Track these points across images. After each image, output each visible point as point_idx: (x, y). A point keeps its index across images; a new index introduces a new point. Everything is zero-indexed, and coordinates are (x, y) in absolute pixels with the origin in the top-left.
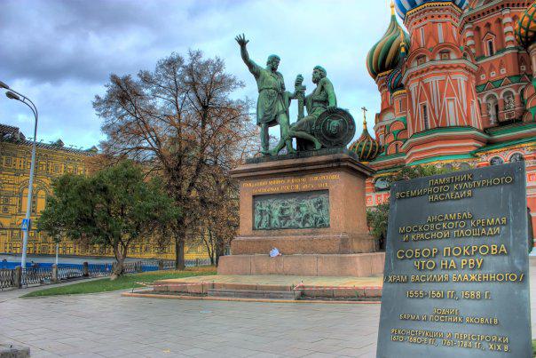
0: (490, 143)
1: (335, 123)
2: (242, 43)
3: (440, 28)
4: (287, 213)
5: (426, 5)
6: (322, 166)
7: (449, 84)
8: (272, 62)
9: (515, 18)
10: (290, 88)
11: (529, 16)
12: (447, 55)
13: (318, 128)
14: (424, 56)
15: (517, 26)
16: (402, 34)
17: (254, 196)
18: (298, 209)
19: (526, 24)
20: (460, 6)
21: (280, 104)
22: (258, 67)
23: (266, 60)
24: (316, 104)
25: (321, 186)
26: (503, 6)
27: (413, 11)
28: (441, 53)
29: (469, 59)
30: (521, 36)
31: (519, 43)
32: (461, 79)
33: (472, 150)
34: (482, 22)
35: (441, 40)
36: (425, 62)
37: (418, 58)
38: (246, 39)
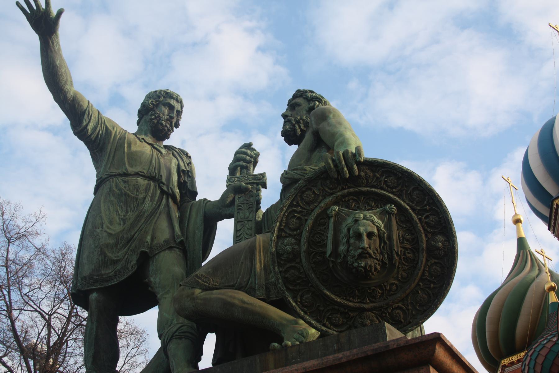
2: (44, 24)
10: (211, 187)
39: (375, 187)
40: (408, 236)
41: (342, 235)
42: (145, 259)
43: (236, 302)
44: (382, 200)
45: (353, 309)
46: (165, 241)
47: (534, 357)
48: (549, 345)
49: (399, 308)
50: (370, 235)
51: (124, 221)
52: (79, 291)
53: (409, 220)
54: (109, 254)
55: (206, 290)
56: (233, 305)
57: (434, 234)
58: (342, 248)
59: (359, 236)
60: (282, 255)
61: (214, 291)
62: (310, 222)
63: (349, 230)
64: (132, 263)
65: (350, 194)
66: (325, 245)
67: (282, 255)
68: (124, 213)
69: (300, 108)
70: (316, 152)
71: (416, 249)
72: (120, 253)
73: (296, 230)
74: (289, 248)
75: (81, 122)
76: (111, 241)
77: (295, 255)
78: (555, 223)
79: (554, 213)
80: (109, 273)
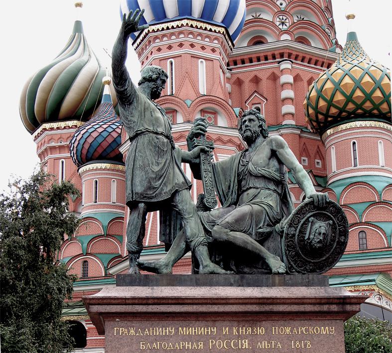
1: (320, 228)
3: (202, 67)
5: (184, 22)
8: (157, 78)
9: (297, 78)
11: (333, 82)
12: (212, 116)
15: (314, 93)
16: (93, 59)
19: (329, 94)
20: (232, 38)
24: (260, 183)
26: (282, 55)
27: (160, 27)
28: (203, 111)
30: (316, 108)
31: (311, 121)
34: (246, 72)
35: (203, 90)
39: (328, 212)
40: (333, 235)
41: (312, 231)
42: (177, 192)
43: (249, 242)
44: (329, 218)
45: (307, 261)
47: (85, 136)
48: (100, 130)
49: (322, 263)
50: (324, 234)
54: (152, 183)
55: (231, 231)
56: (248, 243)
57: (342, 235)
58: (312, 237)
59: (320, 234)
60: (289, 235)
61: (237, 233)
62: (302, 222)
63: (316, 230)
64: (164, 191)
65: (318, 213)
66: (306, 234)
67: (289, 235)
68: (157, 158)
69: (255, 123)
70: (271, 160)
71: (333, 241)
72: (157, 183)
73: (296, 225)
74: (292, 232)
75: (123, 85)
76: (154, 176)
77: (294, 235)
78: (140, 43)
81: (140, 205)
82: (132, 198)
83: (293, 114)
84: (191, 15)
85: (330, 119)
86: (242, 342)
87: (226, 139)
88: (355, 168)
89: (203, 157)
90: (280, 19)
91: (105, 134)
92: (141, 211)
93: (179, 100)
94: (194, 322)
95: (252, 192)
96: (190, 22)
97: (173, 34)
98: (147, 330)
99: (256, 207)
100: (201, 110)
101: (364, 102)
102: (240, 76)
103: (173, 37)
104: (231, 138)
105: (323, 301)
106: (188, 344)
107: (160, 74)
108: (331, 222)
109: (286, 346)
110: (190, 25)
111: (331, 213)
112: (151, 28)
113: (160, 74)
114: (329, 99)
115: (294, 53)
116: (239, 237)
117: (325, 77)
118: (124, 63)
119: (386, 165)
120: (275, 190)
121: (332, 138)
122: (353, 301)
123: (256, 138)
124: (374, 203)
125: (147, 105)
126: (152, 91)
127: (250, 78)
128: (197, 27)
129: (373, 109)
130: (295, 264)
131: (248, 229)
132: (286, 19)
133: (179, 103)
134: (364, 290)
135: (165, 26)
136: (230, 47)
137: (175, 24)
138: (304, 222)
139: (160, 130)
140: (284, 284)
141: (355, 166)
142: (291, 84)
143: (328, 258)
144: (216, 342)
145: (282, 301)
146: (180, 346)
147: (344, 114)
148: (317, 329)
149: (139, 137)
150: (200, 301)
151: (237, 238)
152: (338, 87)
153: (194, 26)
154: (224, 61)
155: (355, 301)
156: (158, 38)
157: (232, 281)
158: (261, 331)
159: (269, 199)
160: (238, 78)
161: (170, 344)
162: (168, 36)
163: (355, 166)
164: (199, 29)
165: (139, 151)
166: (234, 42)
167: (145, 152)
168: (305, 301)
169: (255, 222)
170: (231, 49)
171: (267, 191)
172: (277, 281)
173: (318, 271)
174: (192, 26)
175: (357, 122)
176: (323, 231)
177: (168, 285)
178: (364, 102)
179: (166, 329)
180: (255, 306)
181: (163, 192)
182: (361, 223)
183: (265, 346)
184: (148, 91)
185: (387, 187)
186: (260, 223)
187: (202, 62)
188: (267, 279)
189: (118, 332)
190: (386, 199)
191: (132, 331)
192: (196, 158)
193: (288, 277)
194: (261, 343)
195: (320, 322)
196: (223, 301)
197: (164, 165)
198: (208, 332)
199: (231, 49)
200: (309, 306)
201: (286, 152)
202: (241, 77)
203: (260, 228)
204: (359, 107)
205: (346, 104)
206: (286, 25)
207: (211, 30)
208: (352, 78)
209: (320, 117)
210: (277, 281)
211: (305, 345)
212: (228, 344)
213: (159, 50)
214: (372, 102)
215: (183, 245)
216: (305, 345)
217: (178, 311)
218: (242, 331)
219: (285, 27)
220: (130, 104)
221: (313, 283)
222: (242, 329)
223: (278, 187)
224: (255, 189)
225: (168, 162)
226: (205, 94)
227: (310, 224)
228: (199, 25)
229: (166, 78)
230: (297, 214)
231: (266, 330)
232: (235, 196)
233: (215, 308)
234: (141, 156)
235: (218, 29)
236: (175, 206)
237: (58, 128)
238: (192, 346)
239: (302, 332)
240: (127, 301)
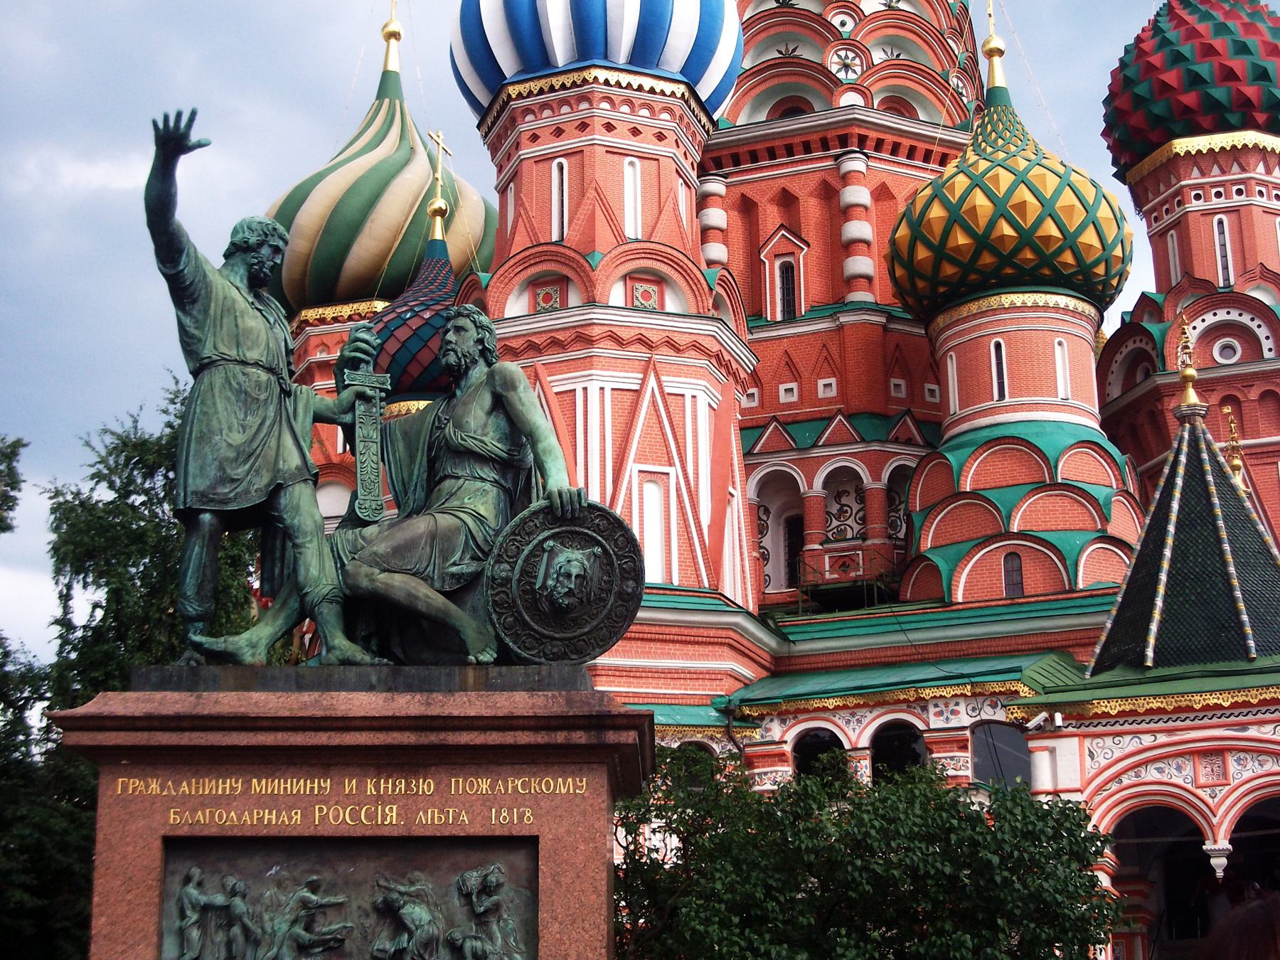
0: (780, 667)
1: (573, 559)
2: (172, 143)
3: (632, 178)
4: (329, 926)
6: (524, 738)
7: (654, 402)
9: (882, 193)
11: (945, 204)
12: (652, 288)
13: (503, 570)
14: (563, 281)
15: (903, 231)
16: (421, 160)
17: (176, 846)
18: (390, 913)
19: (938, 229)
20: (707, 108)
21: (288, 440)
22: (198, 264)
23: (225, 245)
25: (501, 820)
26: (843, 141)
27: (534, 86)
29: (732, 325)
32: (700, 398)
33: (719, 689)
36: (564, 305)
37: (533, 284)
38: (194, 137)
42: (276, 490)
43: (420, 595)
46: (297, 468)
48: (414, 324)
50: (577, 576)
51: (243, 426)
52: (190, 508)
53: (611, 564)
54: (229, 471)
55: (384, 571)
56: (417, 598)
57: (627, 579)
58: (550, 582)
59: (569, 576)
61: (397, 577)
62: (526, 552)
66: (536, 577)
68: (242, 416)
74: (504, 574)
76: (232, 455)
77: (507, 581)
78: (493, 123)
79: (497, 107)
80: (226, 494)
81: (202, 516)
82: (185, 503)
83: (869, 279)
84: (606, 57)
85: (942, 290)
86: (383, 811)
87: (682, 340)
88: (1002, 403)
89: (360, 408)
90: (839, 56)
91: (427, 332)
92: (206, 529)
93: (572, 254)
94: (283, 767)
95: (448, 484)
96: (602, 75)
97: (564, 102)
98: (185, 784)
99: (445, 521)
100: (624, 278)
101: (1017, 251)
102: (747, 190)
103: (565, 109)
104: (695, 338)
105: (553, 723)
106: (270, 813)
107: (266, 235)
108: (598, 550)
109: (479, 818)
110: (602, 81)
111: (600, 532)
112: (513, 91)
113: (266, 235)
114: (936, 243)
115: (873, 135)
116: (399, 583)
117: (928, 192)
118: (173, 215)
119: (1075, 393)
120: (496, 482)
121: (949, 333)
122: (619, 721)
123: (468, 368)
124: (1040, 487)
125: (228, 303)
126: (250, 272)
127: (770, 195)
128: (618, 84)
129: (1039, 266)
130: (515, 643)
131: (424, 565)
132: (853, 59)
133: (570, 258)
134: (994, 694)
135: (542, 83)
136: (703, 127)
137: (567, 79)
138: (531, 554)
139: (252, 355)
140: (488, 686)
141: (1002, 396)
142: (866, 208)
143: (596, 628)
144: (329, 809)
145: (465, 722)
146: (252, 818)
147: (973, 277)
148: (547, 783)
149: (206, 372)
150: (289, 724)
151: (393, 587)
152: (958, 216)
153: (613, 83)
154: (690, 160)
155: (625, 721)
156: (533, 112)
157: (374, 679)
158: (425, 786)
159: (478, 498)
160: (743, 195)
161: (232, 813)
162: (555, 106)
163: (1002, 396)
164: (626, 88)
165: (203, 403)
166: (716, 117)
167: (215, 404)
168: (515, 722)
169: (441, 551)
170: (708, 132)
171: (479, 484)
172: (471, 680)
173: (574, 657)
174: (607, 83)
175: (1003, 297)
176: (575, 571)
177: (236, 689)
178: (1017, 251)
179: (224, 783)
180: (407, 734)
181: (253, 489)
182: (1009, 535)
183: (433, 819)
184: (242, 271)
185: (1071, 447)
186: (453, 553)
187: (631, 163)
188: (448, 675)
189: (125, 788)
190: (1071, 477)
191: (154, 786)
192: (346, 413)
193: (494, 671)
194: (426, 813)
195: (556, 768)
196: (341, 724)
197: (259, 430)
198: (312, 789)
199: (708, 132)
200: (526, 733)
201: (520, 399)
202: (748, 191)
203: (454, 564)
204: (1006, 259)
205: (977, 255)
206: (854, 72)
207: (652, 91)
208: (989, 195)
209: (920, 284)
210: (471, 680)
211: (521, 817)
212: (355, 815)
213: (535, 138)
214: (1035, 249)
215: (294, 604)
216: (521, 817)
217: (244, 743)
218: (386, 786)
219: (851, 76)
220: (194, 301)
221: (549, 684)
222: (386, 782)
223: (504, 476)
224: (453, 481)
225: (268, 423)
226: (640, 237)
227: (546, 555)
228: (625, 79)
229: (281, 244)
230: (513, 533)
231: (437, 785)
232: (420, 494)
233: (323, 738)
234: (205, 413)
235: (669, 88)
236: (281, 520)
237: (335, 320)
238: (278, 817)
239: (515, 788)
240: (139, 724)
